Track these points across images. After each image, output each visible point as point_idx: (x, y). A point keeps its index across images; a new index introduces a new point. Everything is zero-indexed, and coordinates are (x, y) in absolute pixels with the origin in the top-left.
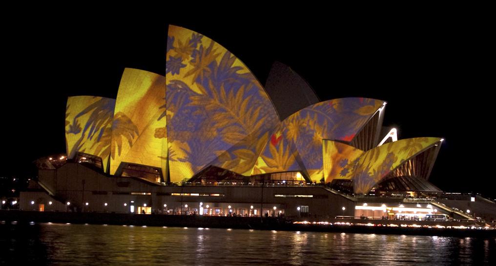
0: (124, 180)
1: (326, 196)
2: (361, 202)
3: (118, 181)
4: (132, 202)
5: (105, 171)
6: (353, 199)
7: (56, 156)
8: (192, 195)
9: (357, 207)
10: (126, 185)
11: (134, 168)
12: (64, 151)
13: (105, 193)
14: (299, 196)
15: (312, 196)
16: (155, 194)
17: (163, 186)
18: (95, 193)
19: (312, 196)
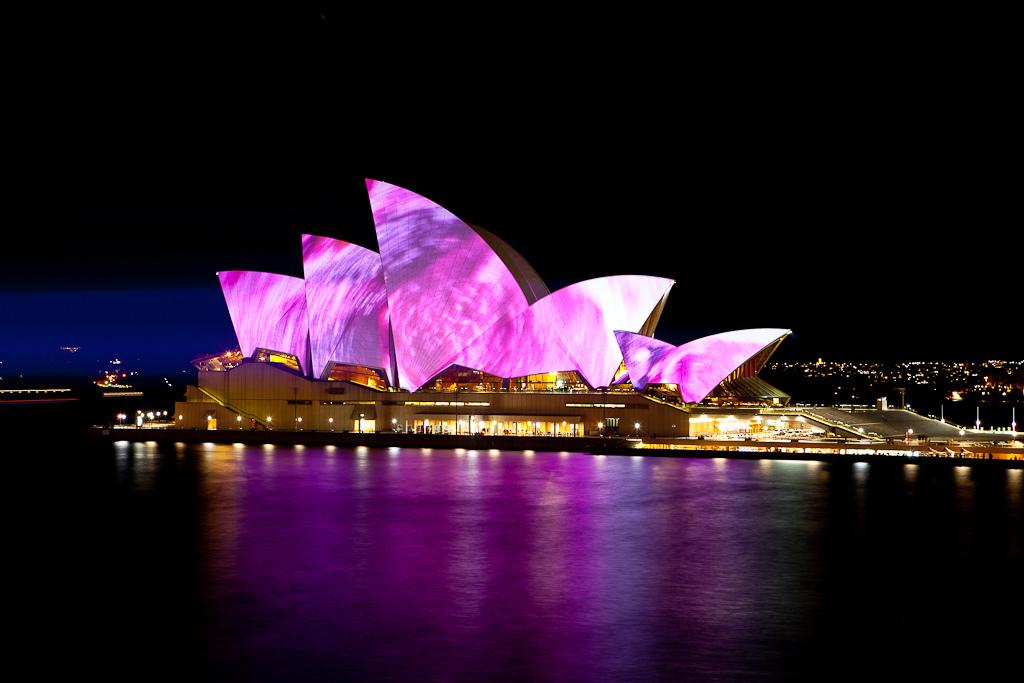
0: (337, 385)
1: (646, 405)
2: (697, 412)
3: (328, 387)
4: (362, 415)
5: (305, 374)
6: (683, 408)
8: (438, 404)
9: (692, 420)
10: (341, 391)
11: (346, 369)
12: (234, 345)
15: (623, 406)
16: (380, 403)
17: (388, 392)
18: (291, 402)
19: (623, 406)
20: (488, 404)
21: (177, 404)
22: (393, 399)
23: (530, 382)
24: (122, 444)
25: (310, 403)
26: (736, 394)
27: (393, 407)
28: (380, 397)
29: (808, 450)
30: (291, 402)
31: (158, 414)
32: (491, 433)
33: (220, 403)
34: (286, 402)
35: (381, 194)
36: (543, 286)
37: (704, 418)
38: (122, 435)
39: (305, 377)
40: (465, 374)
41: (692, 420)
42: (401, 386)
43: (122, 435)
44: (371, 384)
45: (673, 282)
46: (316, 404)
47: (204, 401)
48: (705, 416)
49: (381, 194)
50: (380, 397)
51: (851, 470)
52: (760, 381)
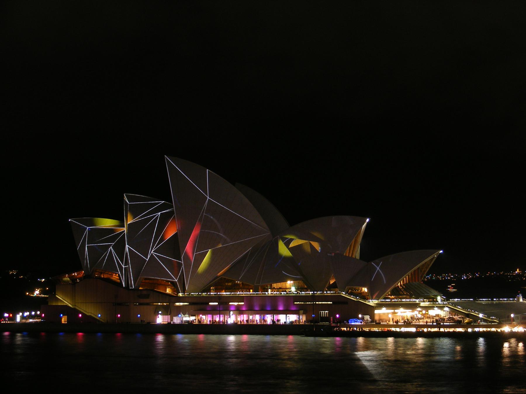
0: (145, 293)
2: (379, 306)
6: (372, 302)
7: (70, 272)
9: (377, 312)
10: (147, 296)
20: (243, 303)
31: (33, 313)
33: (70, 305)
37: (384, 310)
40: (230, 284)
41: (377, 312)
43: (6, 327)
44: (168, 291)
47: (60, 304)
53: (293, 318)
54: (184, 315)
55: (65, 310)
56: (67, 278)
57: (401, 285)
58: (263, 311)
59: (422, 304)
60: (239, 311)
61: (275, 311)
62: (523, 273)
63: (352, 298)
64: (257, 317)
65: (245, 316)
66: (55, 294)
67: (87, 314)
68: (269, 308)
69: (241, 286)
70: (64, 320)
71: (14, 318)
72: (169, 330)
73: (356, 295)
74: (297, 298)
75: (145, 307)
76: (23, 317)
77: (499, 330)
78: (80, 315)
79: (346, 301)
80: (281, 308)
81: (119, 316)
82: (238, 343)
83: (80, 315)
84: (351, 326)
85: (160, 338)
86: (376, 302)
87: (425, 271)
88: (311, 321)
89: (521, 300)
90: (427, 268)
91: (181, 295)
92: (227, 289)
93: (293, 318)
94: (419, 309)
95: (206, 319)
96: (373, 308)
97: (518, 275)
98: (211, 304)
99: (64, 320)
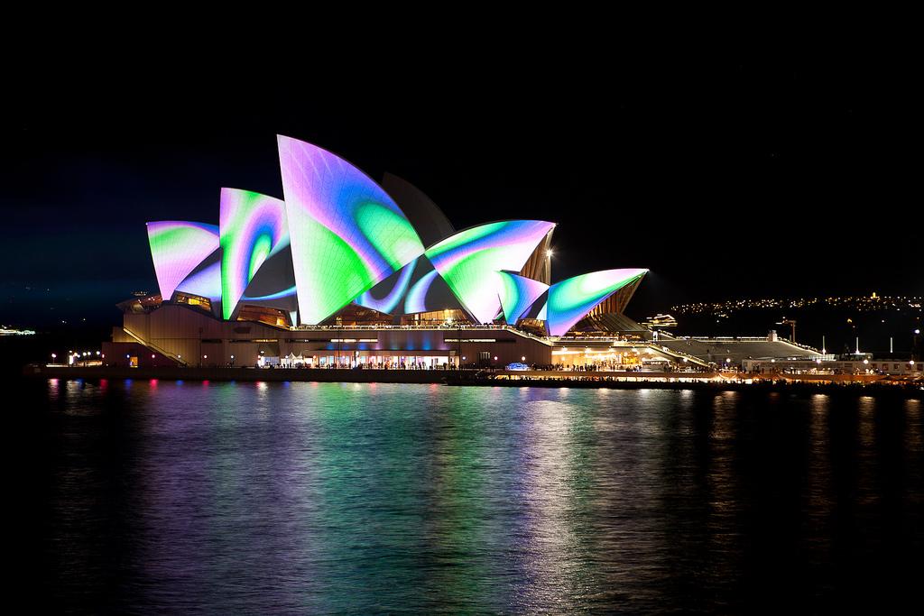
0: (244, 325)
2: (559, 345)
6: (548, 342)
9: (554, 353)
10: (247, 330)
12: (155, 290)
13: (221, 342)
14: (475, 341)
15: (494, 340)
18: (204, 341)
19: (494, 340)
20: (376, 341)
21: (103, 343)
22: (294, 337)
23: (424, 320)
24: (54, 382)
25: (221, 342)
26: (589, 328)
27: (294, 344)
28: (283, 335)
29: (640, 379)
30: (204, 341)
31: (85, 354)
32: (427, 367)
33: (143, 343)
34: (199, 342)
35: (287, 146)
36: (447, 224)
37: (564, 351)
38: (54, 374)
39: (214, 317)
41: (554, 353)
42: (302, 322)
43: (54, 374)
44: (280, 323)
45: (554, 225)
46: (226, 342)
48: (565, 349)
49: (287, 146)
50: (283, 335)
51: (858, 405)
52: (626, 319)
53: (443, 360)
54: (296, 356)
55: (135, 349)
56: (138, 306)
57: (594, 316)
58: (403, 350)
59: (617, 344)
60: (370, 350)
61: (419, 351)
62: (883, 299)
63: (521, 334)
64: (395, 359)
65: (332, 357)
66: (122, 327)
67: (167, 355)
68: (427, 348)
69: (378, 316)
70: (134, 362)
71: (65, 361)
72: (279, 378)
73: (526, 329)
74: (447, 334)
75: (245, 344)
76: (76, 360)
77: (712, 380)
78: (153, 356)
79: (512, 339)
80: (427, 348)
81: (205, 357)
82: (366, 398)
83: (153, 356)
84: (510, 373)
85: (262, 386)
86: (556, 340)
87: (627, 298)
88: (467, 366)
89: (775, 339)
90: (629, 293)
91: (294, 329)
92: (360, 320)
93: (443, 360)
94: (612, 350)
95: (327, 361)
96: (549, 348)
97: (875, 300)
98: (332, 341)
99: (134, 362)
